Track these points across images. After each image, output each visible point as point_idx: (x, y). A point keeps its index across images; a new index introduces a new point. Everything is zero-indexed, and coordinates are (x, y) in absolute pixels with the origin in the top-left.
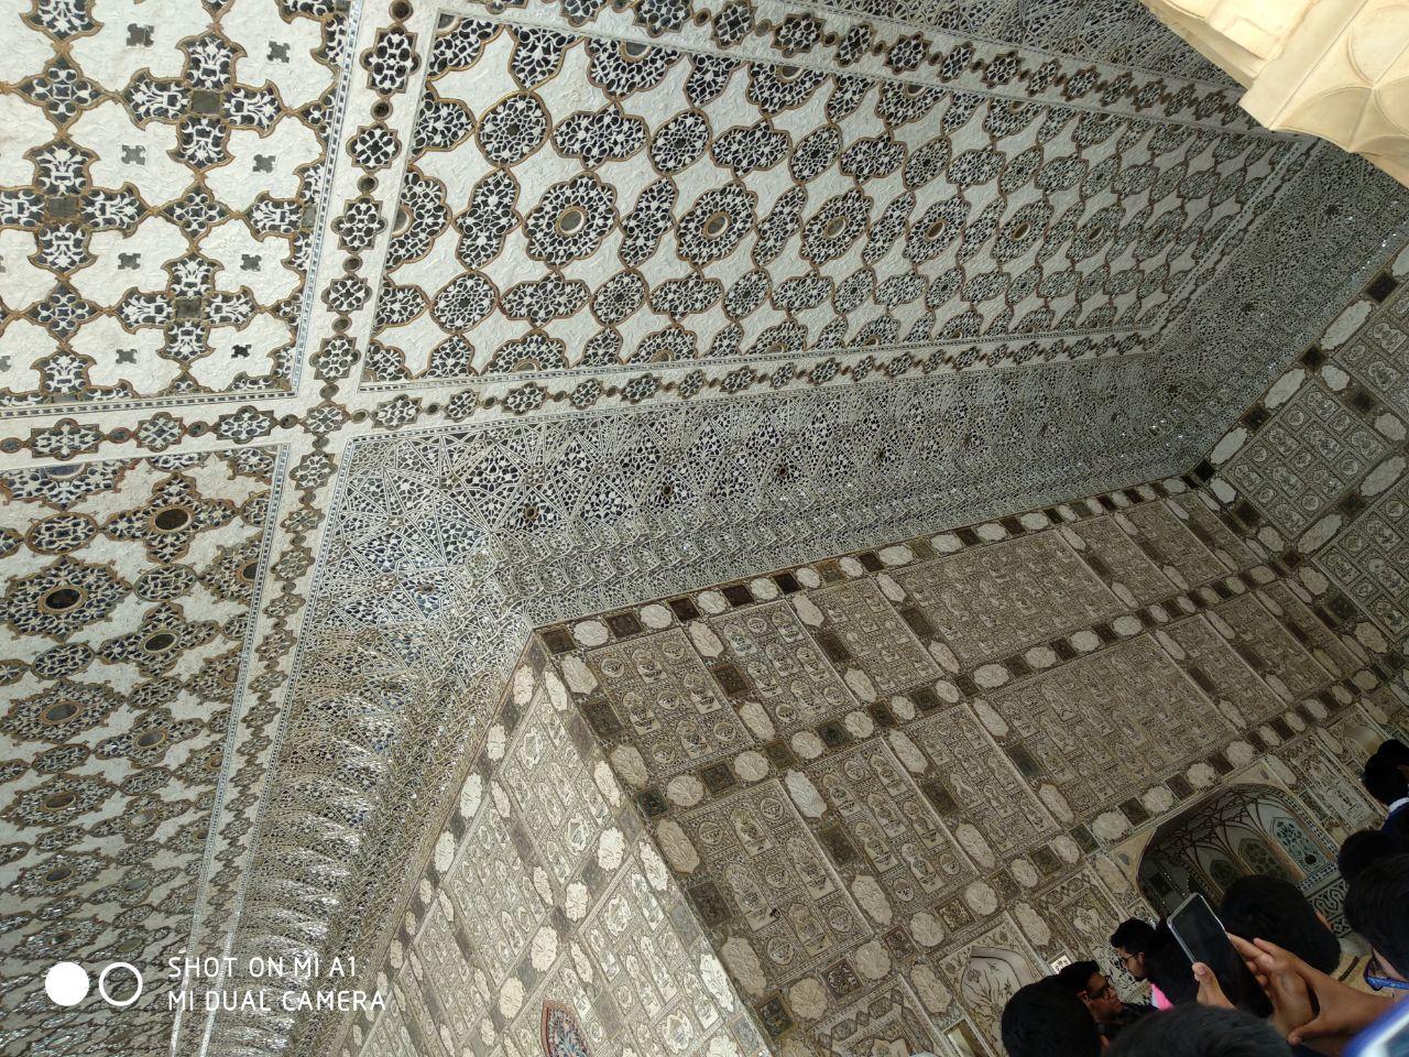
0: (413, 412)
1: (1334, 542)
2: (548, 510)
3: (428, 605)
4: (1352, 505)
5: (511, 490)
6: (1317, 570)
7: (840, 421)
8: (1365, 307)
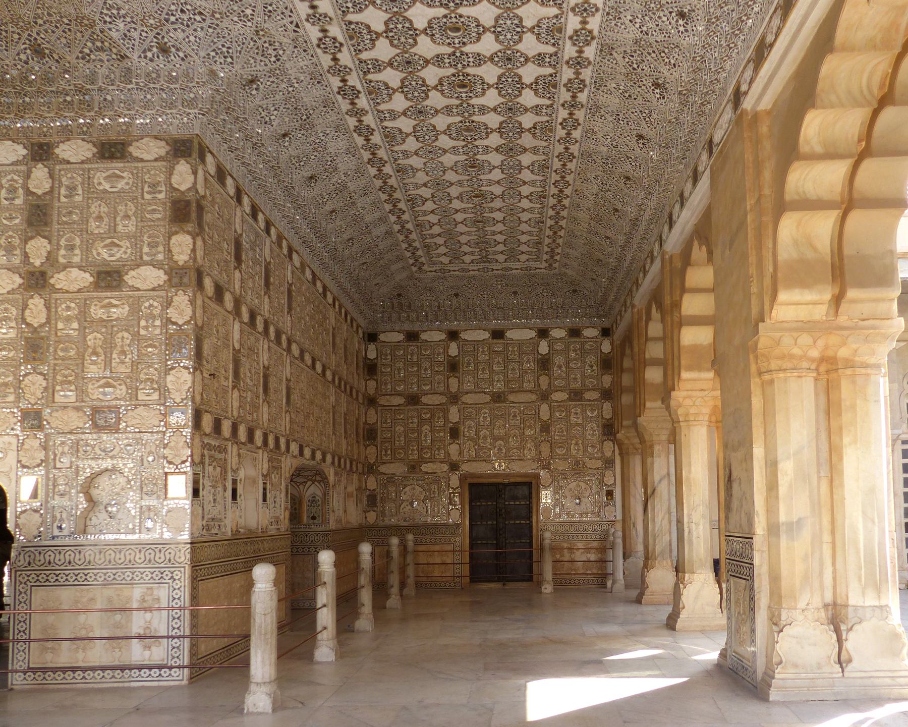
2: (256, 89)
3: (149, 55)
4: (413, 400)
5: (266, 65)
8: (486, 335)
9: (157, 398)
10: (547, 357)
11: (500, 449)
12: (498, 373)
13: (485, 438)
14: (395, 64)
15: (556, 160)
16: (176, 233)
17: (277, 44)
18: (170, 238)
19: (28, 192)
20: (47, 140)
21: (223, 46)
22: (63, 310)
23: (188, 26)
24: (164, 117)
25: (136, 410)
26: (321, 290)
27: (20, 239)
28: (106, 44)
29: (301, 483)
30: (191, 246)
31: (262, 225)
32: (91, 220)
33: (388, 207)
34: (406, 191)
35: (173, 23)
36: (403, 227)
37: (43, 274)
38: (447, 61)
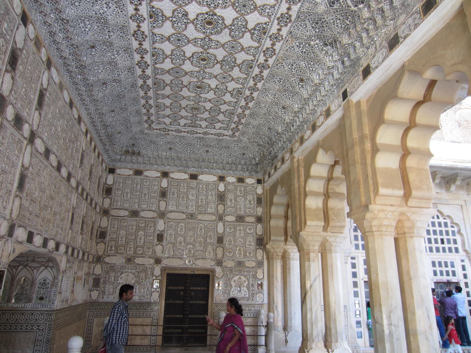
1: (120, 218)
4: (135, 214)
6: (108, 220)
7: (109, 17)
8: (186, 176)
10: (224, 193)
11: (190, 251)
13: (180, 243)
29: (35, 268)
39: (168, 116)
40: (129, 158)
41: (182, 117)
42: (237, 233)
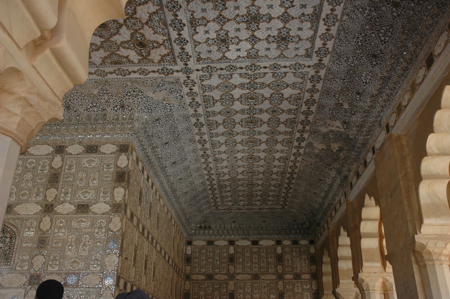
0: (190, 86)
1: (199, 281)
3: (116, 109)
4: (210, 277)
6: (190, 284)
7: (191, 166)
8: (249, 243)
9: (99, 269)
12: (255, 263)
14: (222, 113)
15: (292, 156)
16: (117, 187)
17: (172, 104)
18: (114, 190)
19: (51, 167)
20: (63, 145)
21: (149, 105)
22: (58, 223)
23: (135, 97)
24: (117, 135)
25: (88, 276)
26: (170, 217)
27: (44, 189)
28: (98, 104)
30: (124, 194)
31: (150, 184)
32: (78, 180)
33: (207, 177)
34: (217, 170)
35: (129, 96)
36: (212, 187)
37: (52, 205)
38: (246, 112)
39: (230, 201)
40: (202, 232)
41: (241, 201)
42: (296, 288)
